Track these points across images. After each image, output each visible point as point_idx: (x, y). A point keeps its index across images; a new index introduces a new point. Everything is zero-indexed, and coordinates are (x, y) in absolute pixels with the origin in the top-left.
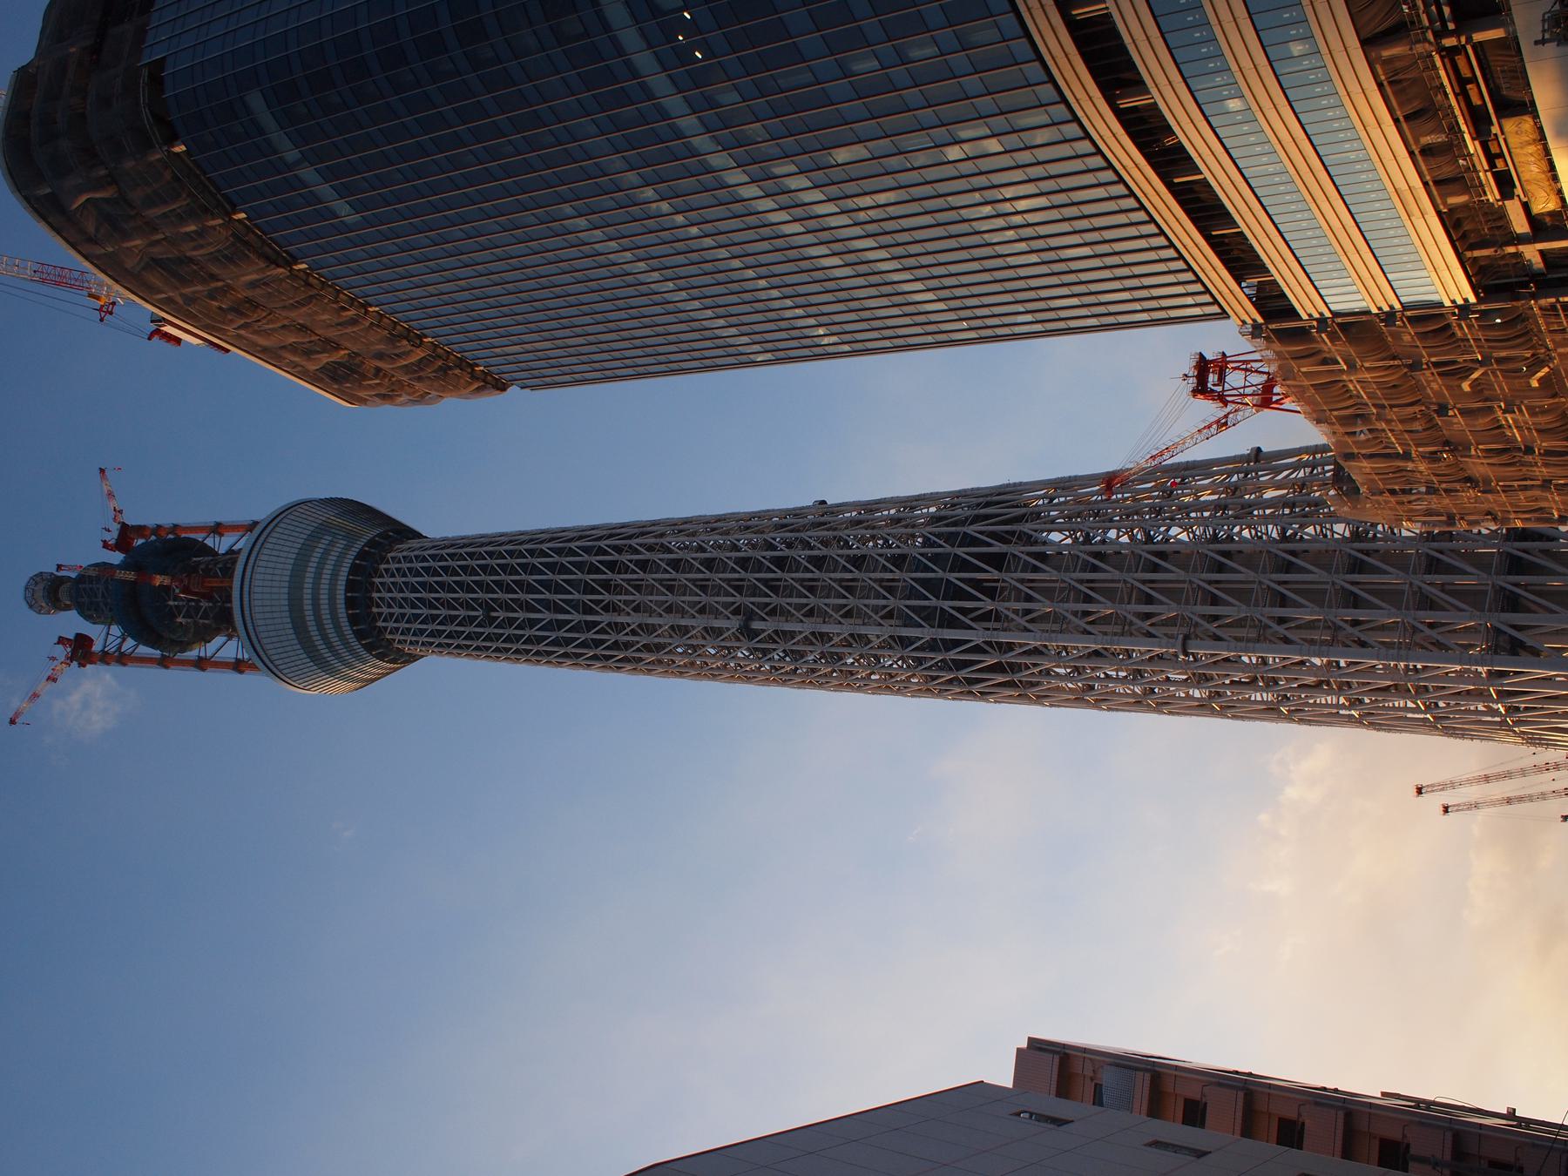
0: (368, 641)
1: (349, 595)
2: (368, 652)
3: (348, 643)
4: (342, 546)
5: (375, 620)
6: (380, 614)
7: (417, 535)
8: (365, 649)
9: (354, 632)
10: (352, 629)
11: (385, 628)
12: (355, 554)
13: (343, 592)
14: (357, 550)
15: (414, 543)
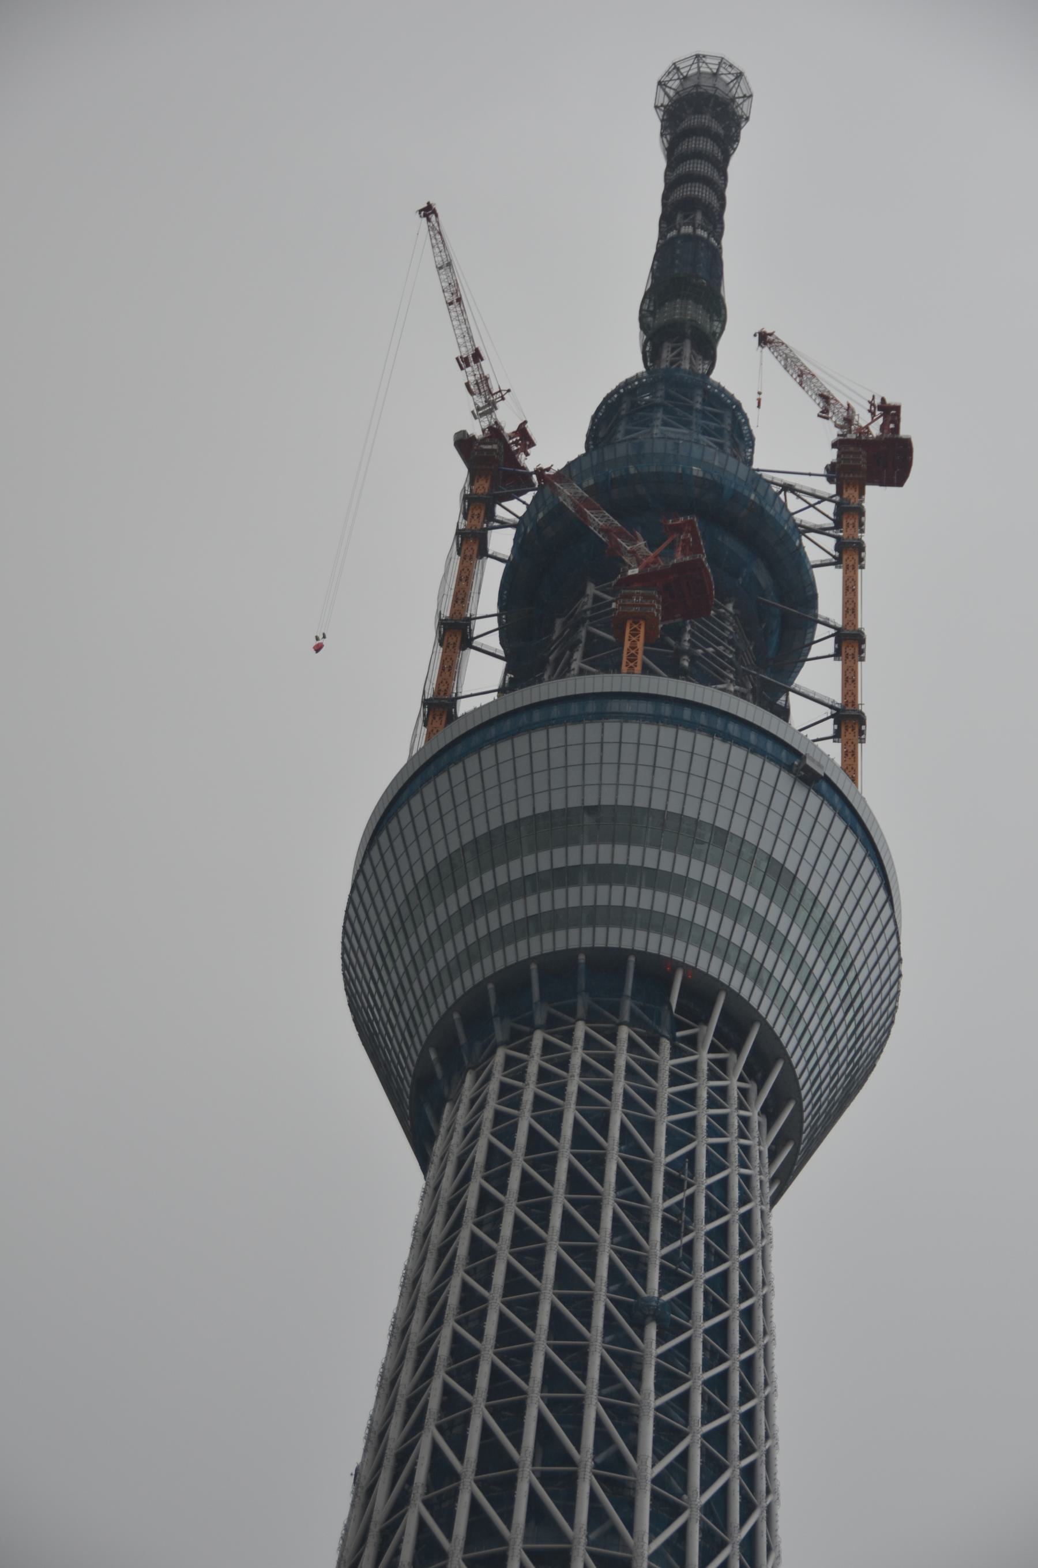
0: (493, 1001)
1: (632, 959)
2: (457, 1002)
3: (492, 950)
4: (768, 965)
5: (551, 1023)
6: (568, 1036)
7: (784, 1178)
8: (476, 987)
9: (521, 968)
10: (530, 960)
11: (526, 1049)
12: (745, 994)
13: (639, 946)
14: (754, 1002)
15: (761, 1172)
